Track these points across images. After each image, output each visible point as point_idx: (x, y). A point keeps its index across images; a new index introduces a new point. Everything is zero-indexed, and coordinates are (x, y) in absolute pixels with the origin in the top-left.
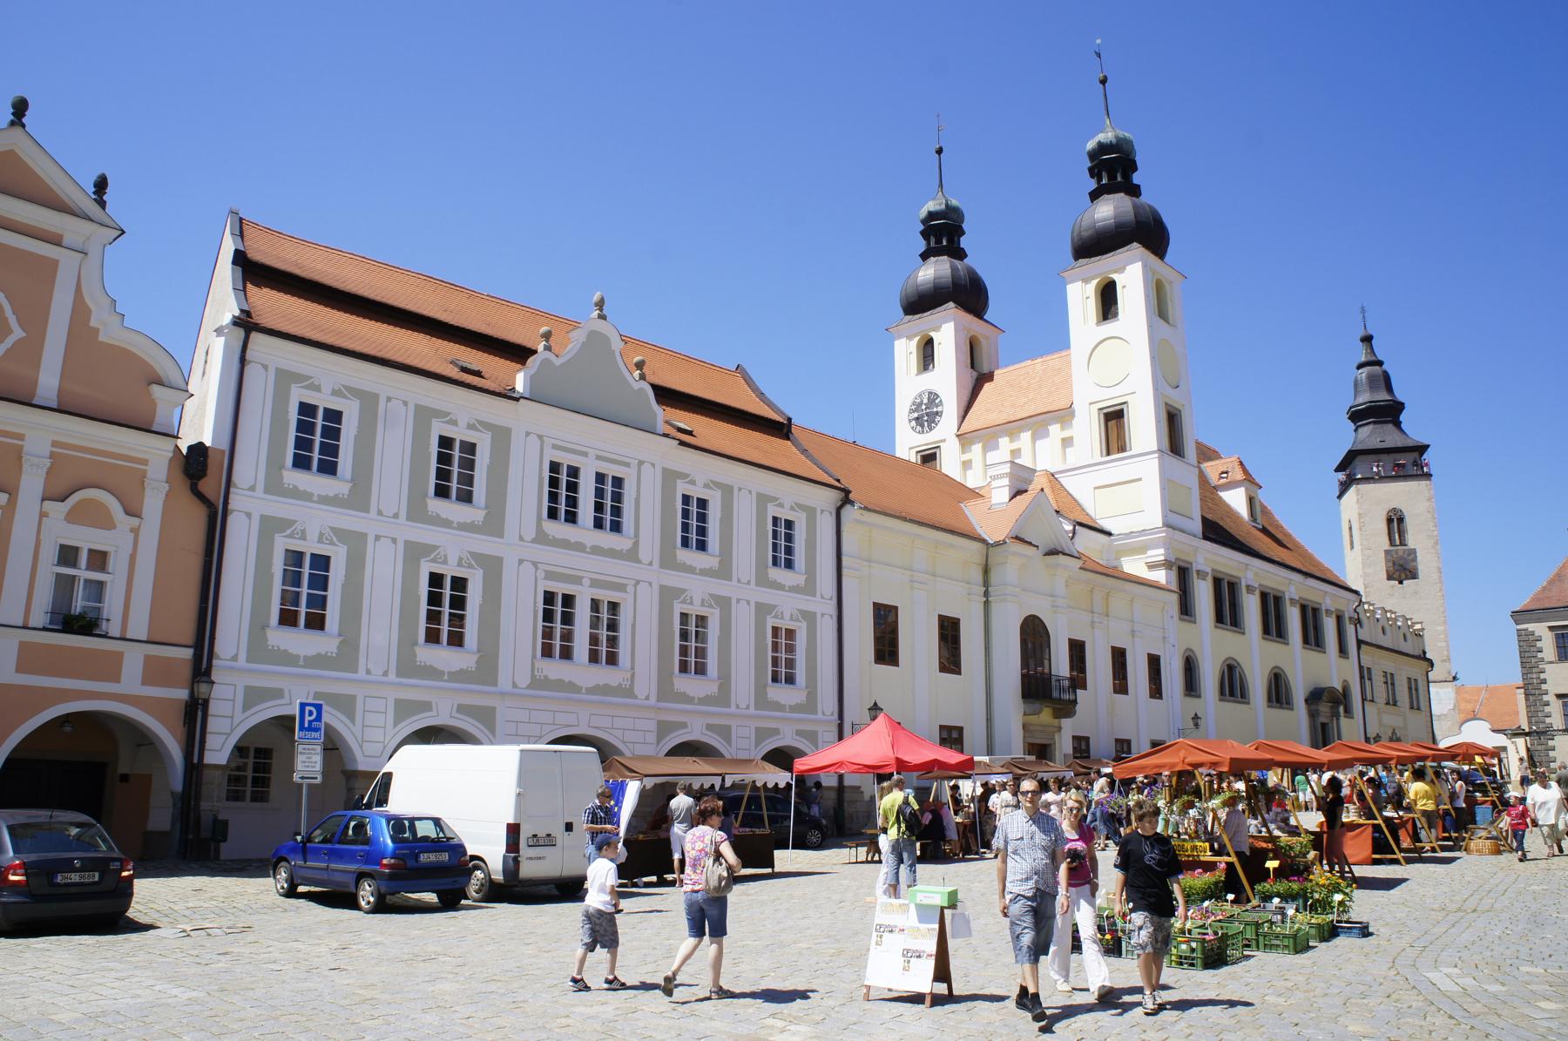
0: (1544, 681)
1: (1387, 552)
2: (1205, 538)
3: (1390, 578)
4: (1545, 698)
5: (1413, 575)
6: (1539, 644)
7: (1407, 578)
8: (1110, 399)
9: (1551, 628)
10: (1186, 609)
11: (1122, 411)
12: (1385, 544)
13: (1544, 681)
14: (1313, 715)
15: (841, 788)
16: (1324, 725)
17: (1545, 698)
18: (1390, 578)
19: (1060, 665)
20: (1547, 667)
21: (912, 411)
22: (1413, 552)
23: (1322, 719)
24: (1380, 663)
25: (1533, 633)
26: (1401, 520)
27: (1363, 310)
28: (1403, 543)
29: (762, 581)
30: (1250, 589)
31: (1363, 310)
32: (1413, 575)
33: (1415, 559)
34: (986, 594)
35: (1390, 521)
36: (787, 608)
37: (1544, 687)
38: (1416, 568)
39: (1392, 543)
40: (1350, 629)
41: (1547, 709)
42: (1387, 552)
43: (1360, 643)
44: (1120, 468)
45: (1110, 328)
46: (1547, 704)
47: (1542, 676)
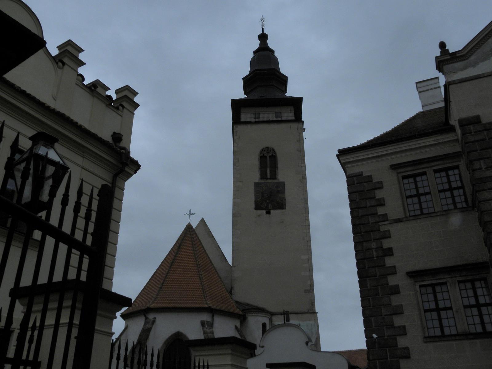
0: (389, 252)
1: (257, 185)
3: (258, 207)
4: (392, 281)
5: (281, 206)
6: (379, 194)
9: (394, 167)
13: (389, 252)
17: (392, 281)
18: (258, 207)
20: (394, 229)
22: (282, 185)
25: (369, 179)
27: (263, 20)
28: (274, 176)
31: (263, 20)
32: (281, 206)
33: (283, 191)
35: (262, 158)
37: (389, 261)
38: (283, 199)
39: (263, 176)
41: (395, 300)
46: (396, 290)
47: (386, 244)
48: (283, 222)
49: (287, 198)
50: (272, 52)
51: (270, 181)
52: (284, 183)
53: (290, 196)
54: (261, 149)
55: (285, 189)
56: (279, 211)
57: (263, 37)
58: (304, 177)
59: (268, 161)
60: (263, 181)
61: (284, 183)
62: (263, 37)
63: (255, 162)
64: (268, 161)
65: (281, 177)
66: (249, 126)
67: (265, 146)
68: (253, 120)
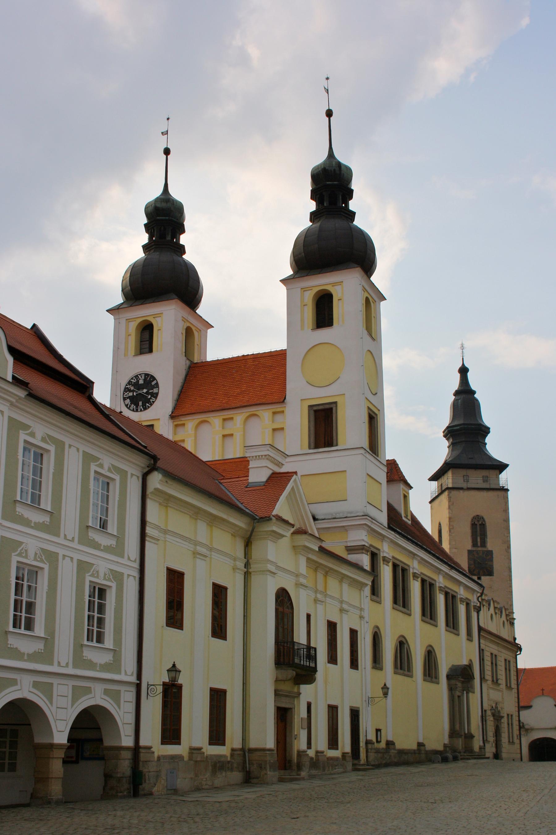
1: (469, 552)
2: (390, 527)
7: (485, 575)
8: (321, 396)
10: (375, 591)
11: (331, 409)
12: (469, 546)
14: (451, 689)
15: (137, 749)
16: (459, 697)
19: (300, 637)
21: (126, 390)
22: (490, 553)
23: (458, 693)
24: (490, 648)
26: (483, 525)
28: (484, 544)
29: (84, 539)
30: (415, 576)
33: (491, 560)
34: (247, 565)
35: (473, 525)
36: (103, 565)
39: (474, 544)
40: (474, 615)
42: (469, 552)
43: (480, 629)
44: (324, 461)
45: (324, 334)
48: (491, 587)
49: (494, 566)
50: (474, 392)
51: (480, 549)
52: (492, 551)
53: (497, 565)
54: (472, 516)
55: (493, 557)
56: (488, 577)
57: (464, 371)
58: (509, 547)
59: (479, 528)
60: (474, 549)
61: (492, 551)
62: (464, 371)
63: (467, 529)
64: (479, 528)
65: (489, 546)
66: (461, 491)
67: (475, 514)
68: (464, 486)
